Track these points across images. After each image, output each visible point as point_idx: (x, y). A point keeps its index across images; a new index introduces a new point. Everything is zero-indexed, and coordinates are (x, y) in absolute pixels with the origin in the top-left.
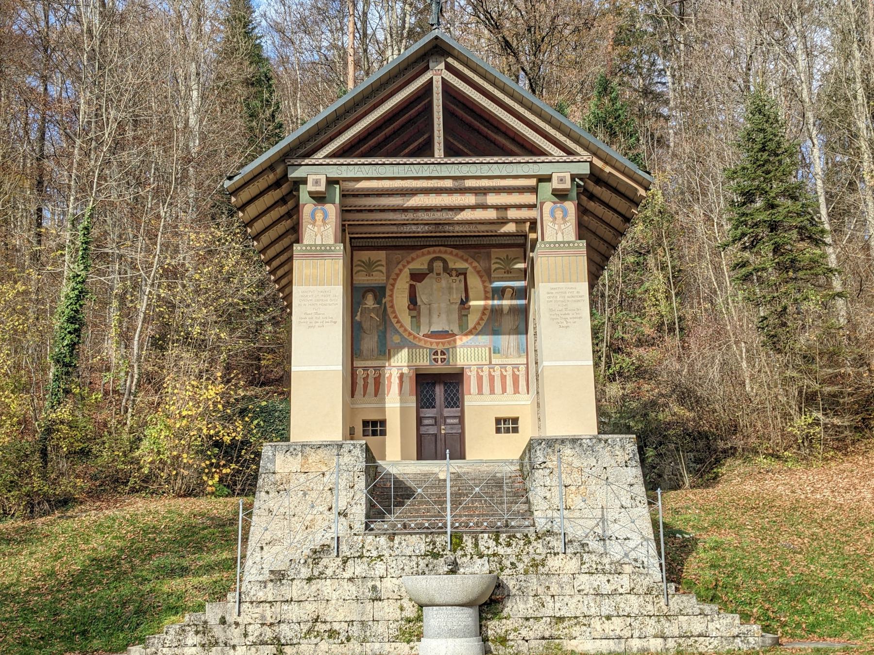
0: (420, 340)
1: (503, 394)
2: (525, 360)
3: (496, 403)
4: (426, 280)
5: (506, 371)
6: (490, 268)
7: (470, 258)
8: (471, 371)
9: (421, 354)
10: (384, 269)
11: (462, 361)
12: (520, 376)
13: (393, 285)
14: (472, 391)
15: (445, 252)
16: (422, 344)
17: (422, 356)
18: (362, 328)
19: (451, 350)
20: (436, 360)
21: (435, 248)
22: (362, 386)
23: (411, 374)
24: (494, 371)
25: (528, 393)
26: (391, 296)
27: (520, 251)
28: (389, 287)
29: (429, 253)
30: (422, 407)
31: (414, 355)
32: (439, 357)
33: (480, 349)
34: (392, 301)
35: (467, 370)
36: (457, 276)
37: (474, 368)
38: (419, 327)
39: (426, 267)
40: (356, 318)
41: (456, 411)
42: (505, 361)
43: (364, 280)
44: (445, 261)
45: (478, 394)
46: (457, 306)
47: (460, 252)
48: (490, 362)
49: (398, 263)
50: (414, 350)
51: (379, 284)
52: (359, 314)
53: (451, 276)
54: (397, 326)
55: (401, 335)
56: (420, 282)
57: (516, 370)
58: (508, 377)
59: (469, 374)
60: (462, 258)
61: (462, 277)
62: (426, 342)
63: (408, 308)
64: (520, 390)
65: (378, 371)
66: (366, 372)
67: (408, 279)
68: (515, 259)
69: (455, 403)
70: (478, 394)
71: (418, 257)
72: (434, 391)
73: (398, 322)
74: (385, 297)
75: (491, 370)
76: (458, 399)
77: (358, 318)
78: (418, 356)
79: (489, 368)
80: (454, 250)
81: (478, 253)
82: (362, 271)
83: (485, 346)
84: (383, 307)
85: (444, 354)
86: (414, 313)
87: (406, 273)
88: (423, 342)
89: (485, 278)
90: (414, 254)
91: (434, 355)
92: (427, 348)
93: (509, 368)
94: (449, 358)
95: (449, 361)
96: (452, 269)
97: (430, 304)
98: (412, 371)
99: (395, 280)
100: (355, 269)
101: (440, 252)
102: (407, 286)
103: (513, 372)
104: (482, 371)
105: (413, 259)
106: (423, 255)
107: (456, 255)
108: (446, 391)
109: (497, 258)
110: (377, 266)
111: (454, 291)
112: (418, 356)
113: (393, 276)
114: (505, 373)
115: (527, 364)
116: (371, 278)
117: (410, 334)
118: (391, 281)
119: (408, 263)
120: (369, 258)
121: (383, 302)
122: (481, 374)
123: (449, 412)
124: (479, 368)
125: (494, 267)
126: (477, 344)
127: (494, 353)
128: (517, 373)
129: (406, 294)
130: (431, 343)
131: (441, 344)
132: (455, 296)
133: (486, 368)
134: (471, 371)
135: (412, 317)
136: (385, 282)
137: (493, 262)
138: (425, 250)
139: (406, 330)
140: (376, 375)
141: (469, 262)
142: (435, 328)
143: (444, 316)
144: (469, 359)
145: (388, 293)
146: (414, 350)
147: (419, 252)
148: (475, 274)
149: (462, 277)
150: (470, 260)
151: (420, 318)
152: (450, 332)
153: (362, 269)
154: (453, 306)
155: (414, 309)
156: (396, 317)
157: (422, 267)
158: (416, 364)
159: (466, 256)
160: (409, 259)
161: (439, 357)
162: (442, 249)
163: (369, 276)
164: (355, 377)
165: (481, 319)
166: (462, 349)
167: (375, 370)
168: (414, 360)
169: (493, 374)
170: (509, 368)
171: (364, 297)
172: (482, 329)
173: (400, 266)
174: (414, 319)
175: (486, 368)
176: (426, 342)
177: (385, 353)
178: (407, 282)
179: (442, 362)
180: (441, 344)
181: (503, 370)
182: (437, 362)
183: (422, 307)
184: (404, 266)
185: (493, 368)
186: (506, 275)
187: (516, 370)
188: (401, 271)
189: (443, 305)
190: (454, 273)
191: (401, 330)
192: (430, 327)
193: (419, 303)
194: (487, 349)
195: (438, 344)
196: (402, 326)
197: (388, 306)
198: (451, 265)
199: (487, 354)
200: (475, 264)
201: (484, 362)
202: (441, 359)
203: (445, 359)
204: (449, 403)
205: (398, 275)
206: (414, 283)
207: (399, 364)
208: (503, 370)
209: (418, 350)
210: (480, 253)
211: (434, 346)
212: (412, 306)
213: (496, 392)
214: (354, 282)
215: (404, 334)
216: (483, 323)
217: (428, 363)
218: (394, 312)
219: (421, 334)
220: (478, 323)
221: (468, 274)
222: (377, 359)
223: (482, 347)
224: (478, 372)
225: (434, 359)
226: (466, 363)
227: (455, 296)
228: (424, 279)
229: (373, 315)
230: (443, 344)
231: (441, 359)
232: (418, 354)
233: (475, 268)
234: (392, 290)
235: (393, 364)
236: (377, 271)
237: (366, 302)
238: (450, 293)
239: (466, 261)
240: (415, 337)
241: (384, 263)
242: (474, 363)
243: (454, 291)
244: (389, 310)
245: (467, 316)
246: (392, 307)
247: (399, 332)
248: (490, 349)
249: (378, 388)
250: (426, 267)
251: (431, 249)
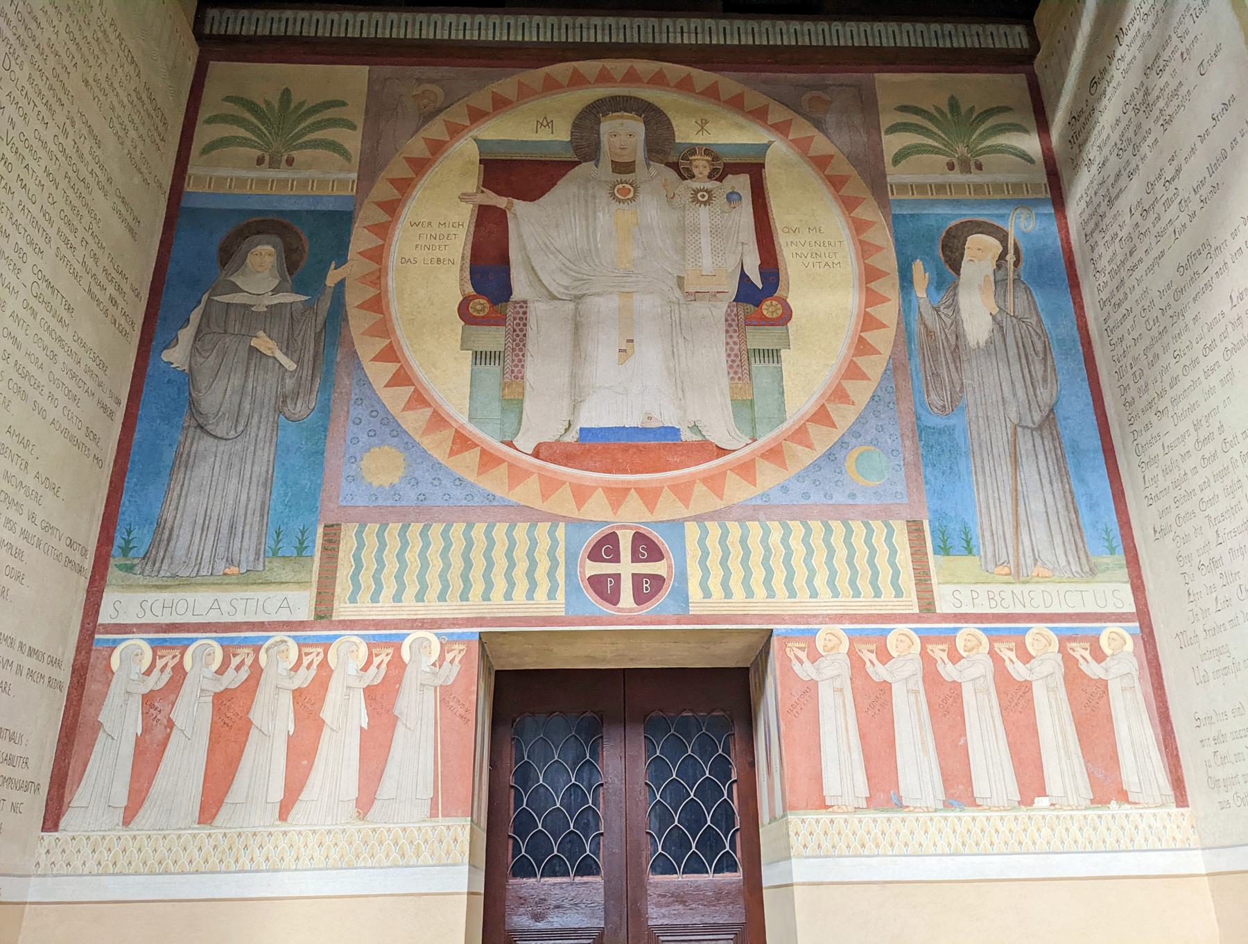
0: (517, 474)
1: (1026, 801)
2: (1126, 590)
3: (993, 866)
4: (564, 189)
5: (1026, 657)
6: (876, 151)
7: (774, 106)
8: (814, 657)
9: (520, 553)
10: (353, 141)
11: (760, 592)
12: (1114, 689)
13: (392, 208)
14: (832, 784)
15: (658, 80)
16: (527, 493)
17: (522, 566)
18: (193, 404)
19: (692, 530)
20: (605, 588)
21: (611, 64)
22: (127, 749)
23: (450, 673)
24: (955, 657)
25: (1181, 798)
26: (377, 255)
27: (1011, 84)
28: (368, 214)
29: (578, 81)
30: (523, 869)
31: (477, 557)
32: (626, 568)
33: (857, 526)
34: (377, 279)
35: (795, 650)
36: (718, 174)
37: (832, 638)
38: (513, 404)
39: (562, 133)
40: (167, 356)
41: (719, 896)
42: (1013, 598)
43: (242, 182)
44: (654, 117)
45: (872, 802)
46: (724, 307)
47: (729, 83)
48: (927, 606)
49: (428, 117)
50: (479, 530)
51: (318, 199)
52: (186, 335)
53: (685, 174)
54: (394, 399)
55: (408, 445)
56: (531, 194)
57: (1080, 651)
58: (1039, 693)
59: (805, 671)
60: (736, 104)
61: (741, 183)
62: (549, 486)
63: (464, 311)
64: (1130, 776)
65: (245, 655)
66: (169, 659)
67: (472, 183)
68: (989, 113)
69: (711, 843)
70: (872, 802)
71: (525, 93)
72: (589, 768)
73: (402, 378)
74: (342, 259)
75: (938, 652)
76: (725, 816)
77: (176, 356)
78: (501, 564)
79: (925, 639)
80: (696, 72)
81: (810, 87)
82: (244, 142)
83: (886, 514)
84: (325, 304)
85: (655, 553)
86: (492, 338)
87: (466, 150)
88: (533, 484)
89: (857, 186)
90: (506, 85)
91: (594, 555)
92: (554, 519)
93: (1040, 638)
94: (683, 577)
95: (682, 596)
96: (692, 150)
97: (578, 299)
98: (457, 651)
99: (404, 186)
100: (204, 134)
101: (631, 77)
102: (464, 215)
103: (1070, 662)
104: (884, 656)
105: (501, 104)
106: (551, 86)
107: (712, 93)
108: (658, 769)
109: (904, 109)
110: (318, 126)
111: (705, 241)
112: (501, 564)
113: (397, 168)
114: (1019, 671)
115: (1143, 615)
116: (283, 174)
117: (462, 442)
118: (382, 190)
119: (477, 116)
120: (287, 92)
121: (332, 278)
122: (879, 672)
123: (680, 897)
124: (864, 637)
125: (892, 143)
126: (840, 498)
127: (943, 549)
128: (1093, 669)
129: (458, 245)
130: (581, 494)
131: (633, 500)
132: (707, 262)
133: (902, 638)
134: (814, 657)
135: (481, 357)
136: (350, 192)
137: (886, 120)
138: (561, 70)
139: (439, 420)
140: (232, 679)
141: (772, 119)
142: (597, 415)
143: (650, 353)
144: (799, 581)
145: (360, 240)
146: (479, 530)
147: (534, 76)
148: (807, 170)
149: (741, 183)
150: (778, 114)
151: (520, 363)
152: (687, 436)
153: (242, 132)
154: (700, 308)
155: (495, 320)
156: (390, 354)
157: (544, 135)
158: (485, 610)
159: (755, 99)
160: (481, 99)
161: (626, 568)
162: (645, 67)
163: (274, 164)
164: (92, 687)
165: (853, 372)
166: (754, 528)
167: (156, 646)
168: (478, 588)
169: (949, 671)
170: (1040, 638)
171: (229, 254)
172: (861, 420)
173: (435, 129)
174: (495, 369)
175: (902, 638)
176: (549, 486)
177: (302, 548)
178: (464, 197)
179: (640, 598)
180: (633, 500)
181: (1008, 654)
182: (613, 598)
183: (538, 310)
184: (455, 131)
185: (948, 638)
186: (957, 177)
187: (1080, 651)
188: (437, 148)
189: (646, 303)
190: (701, 165)
191: (413, 421)
192: (575, 407)
193: (521, 286)
194: (900, 527)
195: (617, 495)
196: (419, 399)
197: (353, 299)
198: (686, 132)
199: (904, 557)
200: (801, 129)
201: (888, 603)
202: (637, 578)
203: (658, 581)
204: (678, 843)
205: (420, 166)
206: (501, 202)
207: (384, 610)
208: (1007, 653)
209: (500, 530)
210: (824, 88)
211: (598, 510)
212: (481, 306)
213: (981, 787)
214: (190, 187)
215: (426, 442)
216: (861, 392)
217: (558, 607)
218: (383, 328)
219: (526, 442)
220: (839, 394)
221: (769, 172)
222: (249, 579)
223: (867, 516)
224: (857, 664)
225: (597, 583)
226: (782, 604)
227: (707, 262)
228: (551, 183)
229: (263, 342)
230: (650, 497)
231: (637, 578)
232: (499, 553)
233: (802, 146)
234: (383, 231)
235: (343, 609)
236: (315, 144)
237: (238, 280)
238: (682, 250)
239: (759, 115)
240: (489, 460)
241: (355, 112)
242: (826, 603)
243: (705, 241)
244: (358, 322)
245: (773, 355)
246: (377, 304)
247: (397, 431)
248: (915, 528)
249: (233, 764)
250: (566, 137)
251: (590, 67)
